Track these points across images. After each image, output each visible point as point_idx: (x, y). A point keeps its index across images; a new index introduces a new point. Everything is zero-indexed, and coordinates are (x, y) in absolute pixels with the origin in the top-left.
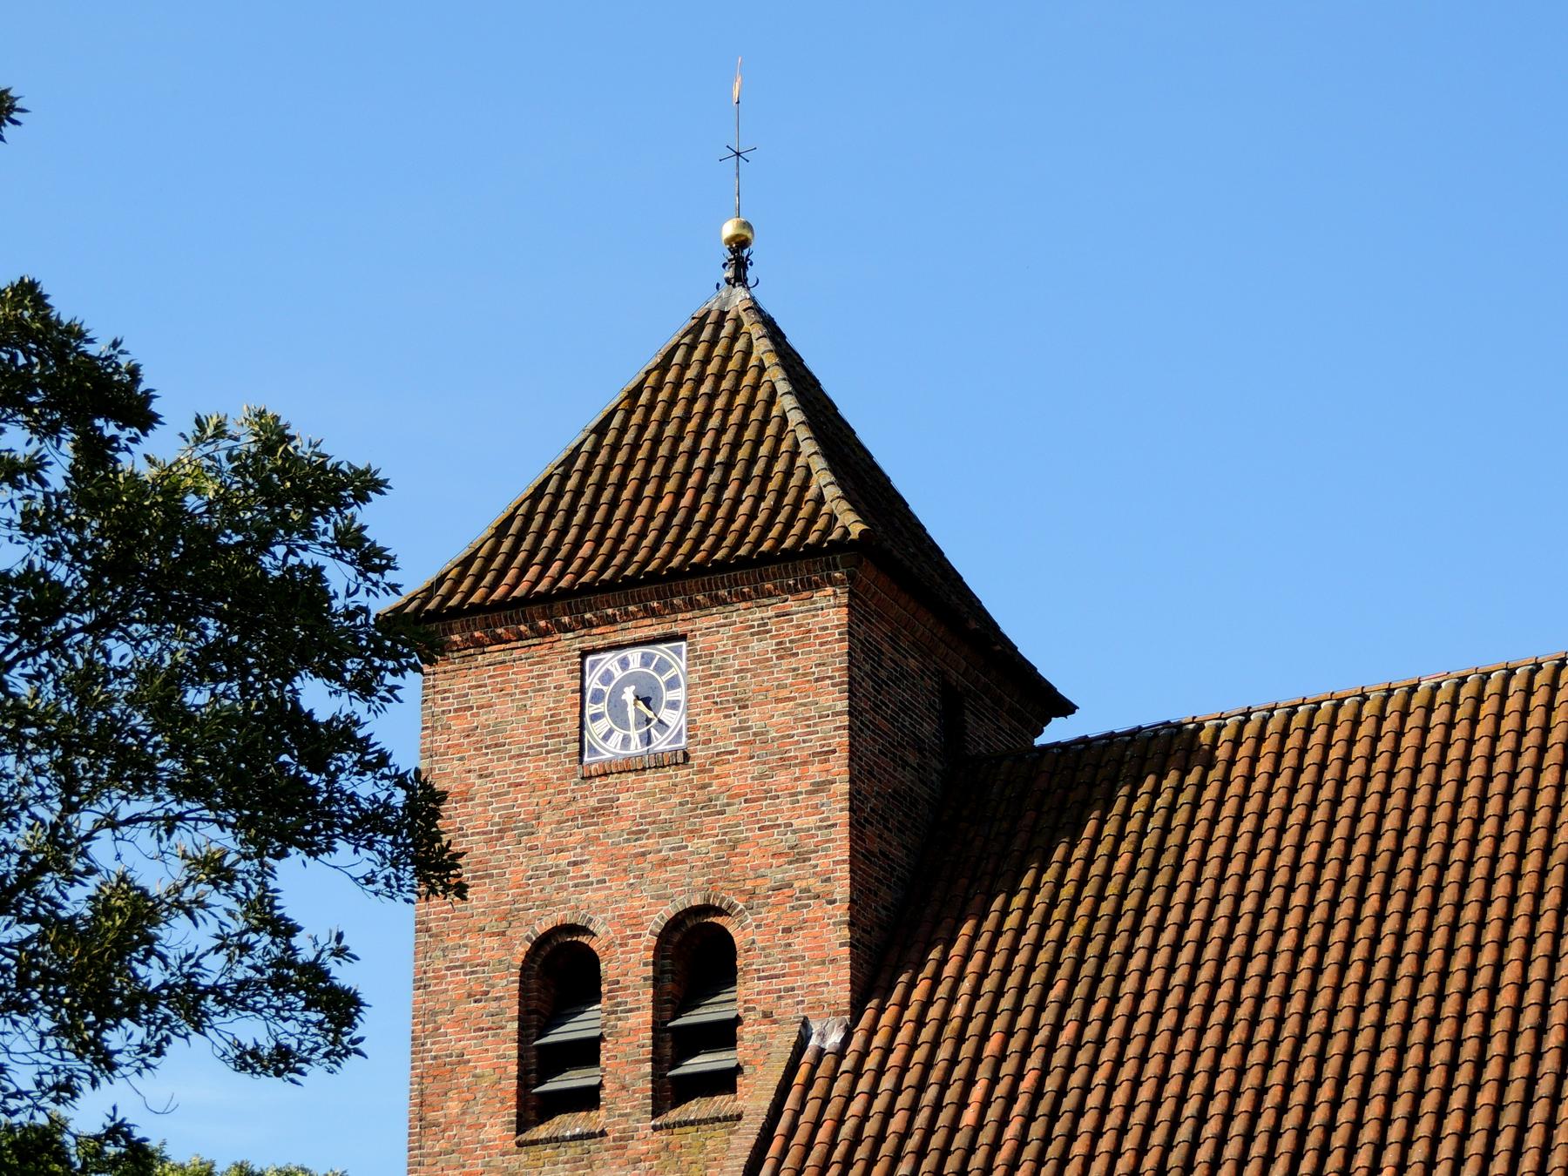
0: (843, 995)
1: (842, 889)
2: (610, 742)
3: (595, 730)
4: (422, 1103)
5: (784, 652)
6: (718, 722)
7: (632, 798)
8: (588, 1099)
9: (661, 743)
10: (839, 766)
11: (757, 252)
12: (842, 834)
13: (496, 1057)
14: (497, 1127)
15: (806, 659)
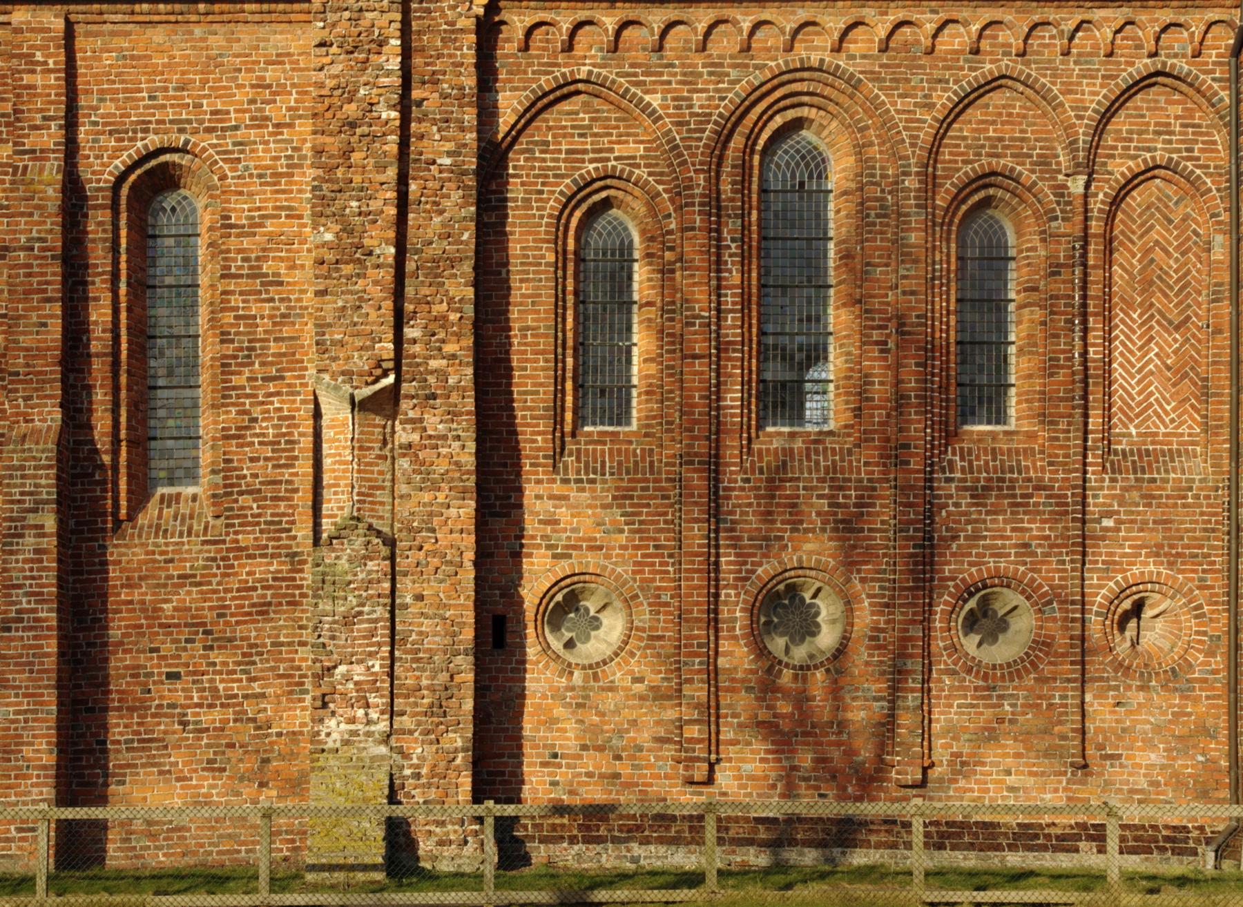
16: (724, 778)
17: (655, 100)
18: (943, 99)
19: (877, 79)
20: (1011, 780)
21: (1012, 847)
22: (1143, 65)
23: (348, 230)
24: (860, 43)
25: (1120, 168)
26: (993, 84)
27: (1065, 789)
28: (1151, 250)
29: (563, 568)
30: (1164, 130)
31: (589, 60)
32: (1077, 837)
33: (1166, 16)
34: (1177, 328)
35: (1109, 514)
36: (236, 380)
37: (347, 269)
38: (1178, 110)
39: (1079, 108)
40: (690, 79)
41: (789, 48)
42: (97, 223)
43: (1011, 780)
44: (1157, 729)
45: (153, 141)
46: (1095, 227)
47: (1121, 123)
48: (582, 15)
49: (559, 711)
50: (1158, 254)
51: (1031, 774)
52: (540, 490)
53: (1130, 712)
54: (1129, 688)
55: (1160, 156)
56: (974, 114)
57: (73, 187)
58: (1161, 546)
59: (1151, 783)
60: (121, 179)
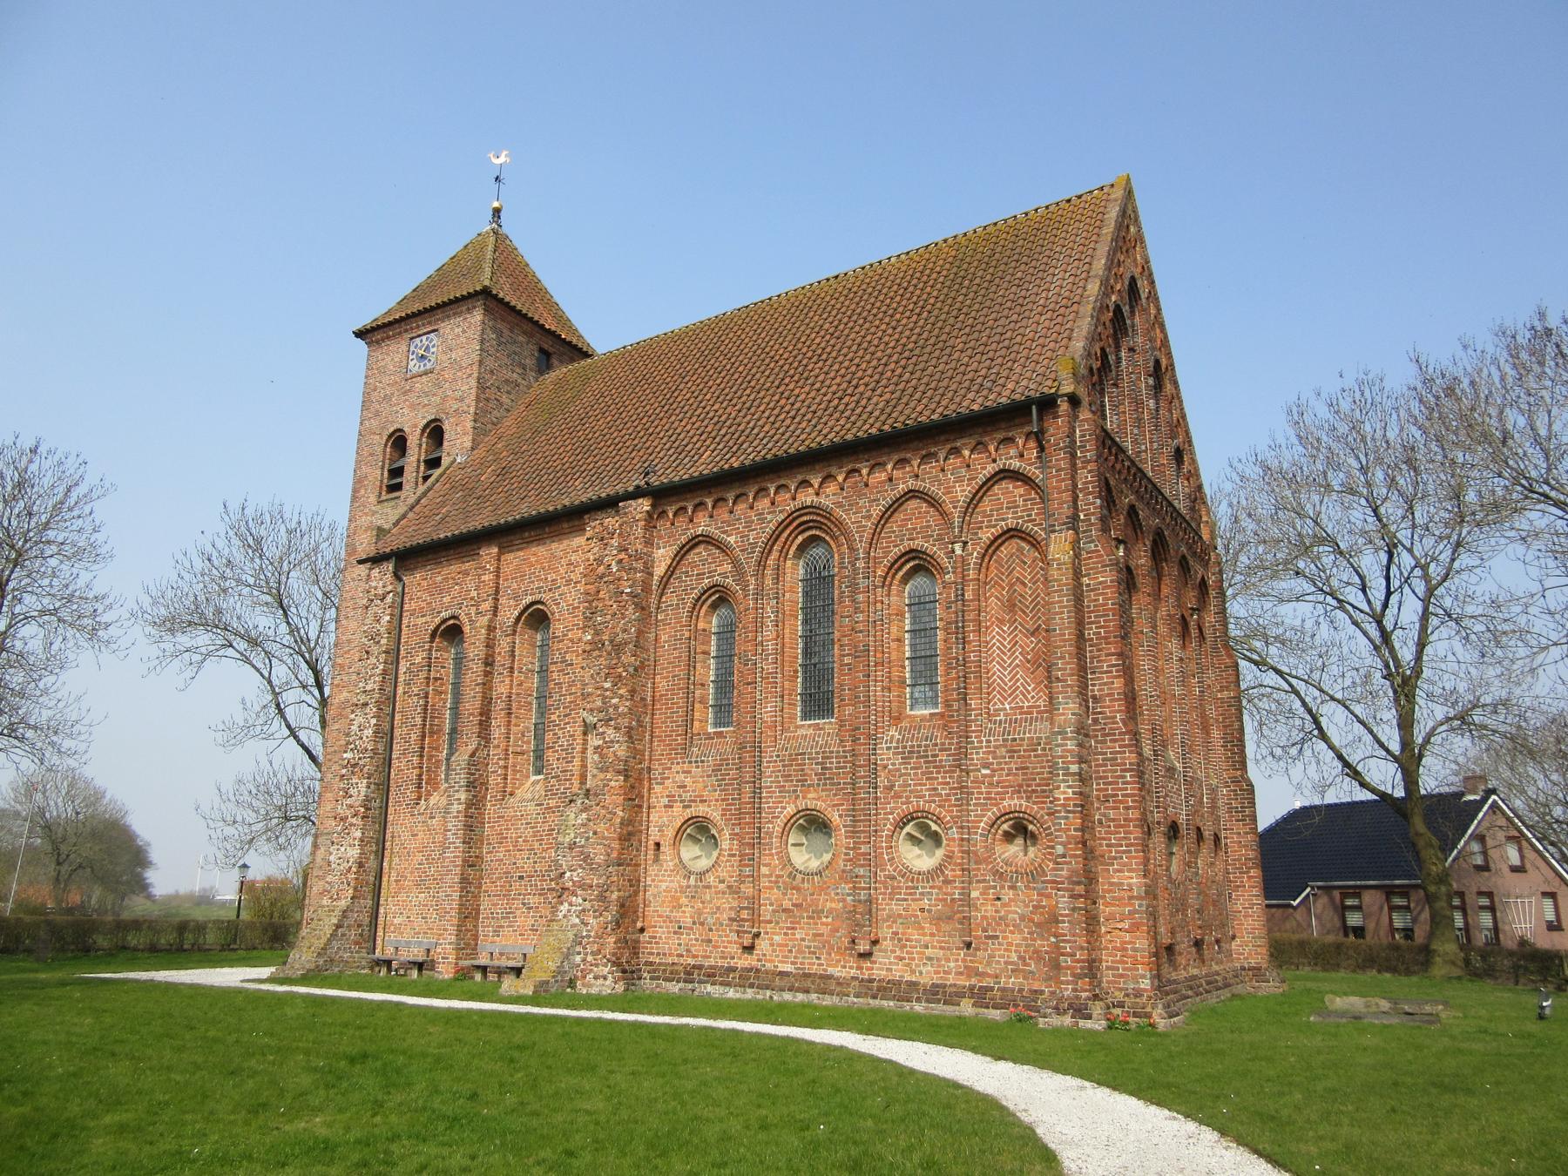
0: (468, 444)
1: (472, 410)
2: (415, 366)
3: (412, 364)
4: (355, 491)
5: (464, 332)
6: (445, 358)
7: (421, 384)
8: (399, 487)
9: (429, 366)
10: (475, 367)
11: (502, 214)
12: (474, 391)
13: (376, 475)
14: (373, 499)
15: (470, 333)
16: (763, 945)
17: (732, 539)
18: (876, 512)
19: (840, 505)
20: (929, 952)
21: (918, 1000)
22: (991, 468)
23: (597, 633)
24: (831, 488)
25: (986, 535)
26: (912, 494)
27: (964, 961)
28: (1012, 585)
29: (688, 813)
30: (1013, 506)
31: (703, 525)
32: (961, 995)
33: (1000, 436)
34: (1033, 634)
35: (986, 766)
36: (553, 717)
37: (596, 653)
38: (1021, 491)
39: (954, 502)
40: (749, 523)
41: (794, 499)
42: (503, 644)
43: (929, 952)
44: (1022, 918)
45: (529, 599)
46: (972, 574)
47: (986, 505)
48: (697, 501)
49: (684, 900)
50: (1018, 587)
51: (942, 948)
52: (675, 768)
53: (1004, 905)
54: (1002, 887)
55: (1011, 523)
56: (899, 516)
57: (491, 628)
58: (1020, 786)
59: (1020, 958)
60: (518, 619)
